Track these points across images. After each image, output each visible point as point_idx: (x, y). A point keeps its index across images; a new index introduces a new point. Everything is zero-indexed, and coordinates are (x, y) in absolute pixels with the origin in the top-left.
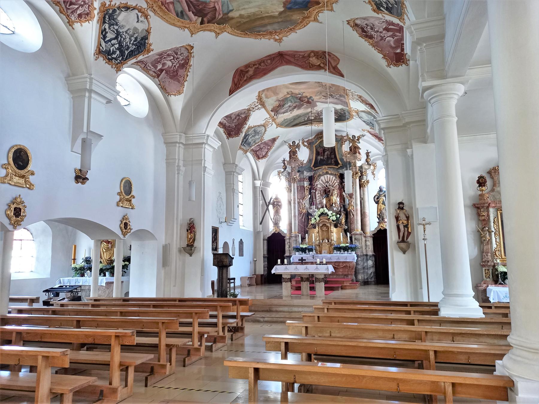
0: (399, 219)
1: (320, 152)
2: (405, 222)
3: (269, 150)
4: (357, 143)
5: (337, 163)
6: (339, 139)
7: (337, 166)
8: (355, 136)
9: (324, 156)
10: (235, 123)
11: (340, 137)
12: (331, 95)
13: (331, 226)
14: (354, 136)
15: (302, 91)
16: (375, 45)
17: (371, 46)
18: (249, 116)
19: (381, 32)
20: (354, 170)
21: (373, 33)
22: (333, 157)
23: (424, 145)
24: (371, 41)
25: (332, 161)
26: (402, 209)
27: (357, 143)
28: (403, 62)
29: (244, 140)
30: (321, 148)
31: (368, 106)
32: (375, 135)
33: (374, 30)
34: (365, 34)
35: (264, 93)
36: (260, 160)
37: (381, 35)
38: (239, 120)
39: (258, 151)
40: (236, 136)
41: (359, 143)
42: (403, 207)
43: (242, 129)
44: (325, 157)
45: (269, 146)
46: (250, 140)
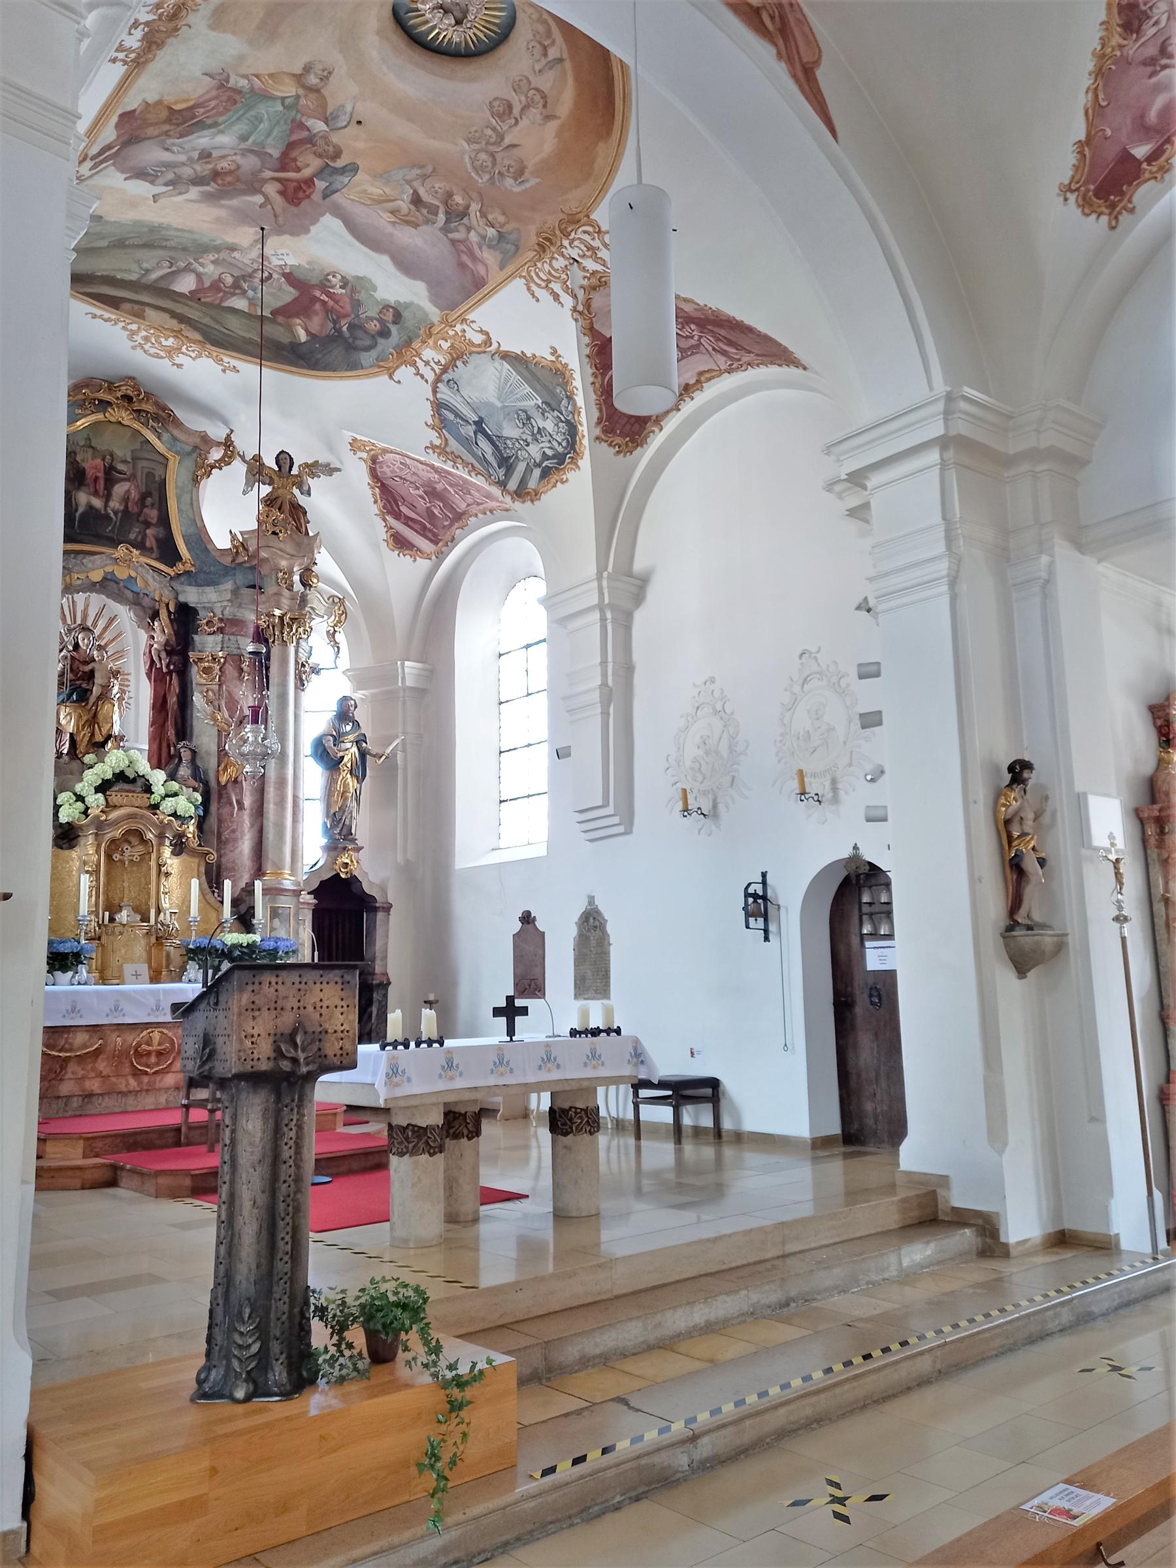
1: (90, 473)
4: (296, 491)
5: (169, 553)
7: (172, 565)
8: (291, 459)
9: (108, 498)
12: (457, 215)
13: (161, 844)
14: (284, 459)
15: (364, 109)
17: (1090, 66)
20: (285, 602)
22: (154, 521)
23: (1077, 554)
24: (1116, 40)
25: (145, 536)
27: (296, 491)
28: (1113, 206)
30: (94, 458)
31: (587, 340)
32: (389, 482)
41: (309, 494)
44: (115, 504)
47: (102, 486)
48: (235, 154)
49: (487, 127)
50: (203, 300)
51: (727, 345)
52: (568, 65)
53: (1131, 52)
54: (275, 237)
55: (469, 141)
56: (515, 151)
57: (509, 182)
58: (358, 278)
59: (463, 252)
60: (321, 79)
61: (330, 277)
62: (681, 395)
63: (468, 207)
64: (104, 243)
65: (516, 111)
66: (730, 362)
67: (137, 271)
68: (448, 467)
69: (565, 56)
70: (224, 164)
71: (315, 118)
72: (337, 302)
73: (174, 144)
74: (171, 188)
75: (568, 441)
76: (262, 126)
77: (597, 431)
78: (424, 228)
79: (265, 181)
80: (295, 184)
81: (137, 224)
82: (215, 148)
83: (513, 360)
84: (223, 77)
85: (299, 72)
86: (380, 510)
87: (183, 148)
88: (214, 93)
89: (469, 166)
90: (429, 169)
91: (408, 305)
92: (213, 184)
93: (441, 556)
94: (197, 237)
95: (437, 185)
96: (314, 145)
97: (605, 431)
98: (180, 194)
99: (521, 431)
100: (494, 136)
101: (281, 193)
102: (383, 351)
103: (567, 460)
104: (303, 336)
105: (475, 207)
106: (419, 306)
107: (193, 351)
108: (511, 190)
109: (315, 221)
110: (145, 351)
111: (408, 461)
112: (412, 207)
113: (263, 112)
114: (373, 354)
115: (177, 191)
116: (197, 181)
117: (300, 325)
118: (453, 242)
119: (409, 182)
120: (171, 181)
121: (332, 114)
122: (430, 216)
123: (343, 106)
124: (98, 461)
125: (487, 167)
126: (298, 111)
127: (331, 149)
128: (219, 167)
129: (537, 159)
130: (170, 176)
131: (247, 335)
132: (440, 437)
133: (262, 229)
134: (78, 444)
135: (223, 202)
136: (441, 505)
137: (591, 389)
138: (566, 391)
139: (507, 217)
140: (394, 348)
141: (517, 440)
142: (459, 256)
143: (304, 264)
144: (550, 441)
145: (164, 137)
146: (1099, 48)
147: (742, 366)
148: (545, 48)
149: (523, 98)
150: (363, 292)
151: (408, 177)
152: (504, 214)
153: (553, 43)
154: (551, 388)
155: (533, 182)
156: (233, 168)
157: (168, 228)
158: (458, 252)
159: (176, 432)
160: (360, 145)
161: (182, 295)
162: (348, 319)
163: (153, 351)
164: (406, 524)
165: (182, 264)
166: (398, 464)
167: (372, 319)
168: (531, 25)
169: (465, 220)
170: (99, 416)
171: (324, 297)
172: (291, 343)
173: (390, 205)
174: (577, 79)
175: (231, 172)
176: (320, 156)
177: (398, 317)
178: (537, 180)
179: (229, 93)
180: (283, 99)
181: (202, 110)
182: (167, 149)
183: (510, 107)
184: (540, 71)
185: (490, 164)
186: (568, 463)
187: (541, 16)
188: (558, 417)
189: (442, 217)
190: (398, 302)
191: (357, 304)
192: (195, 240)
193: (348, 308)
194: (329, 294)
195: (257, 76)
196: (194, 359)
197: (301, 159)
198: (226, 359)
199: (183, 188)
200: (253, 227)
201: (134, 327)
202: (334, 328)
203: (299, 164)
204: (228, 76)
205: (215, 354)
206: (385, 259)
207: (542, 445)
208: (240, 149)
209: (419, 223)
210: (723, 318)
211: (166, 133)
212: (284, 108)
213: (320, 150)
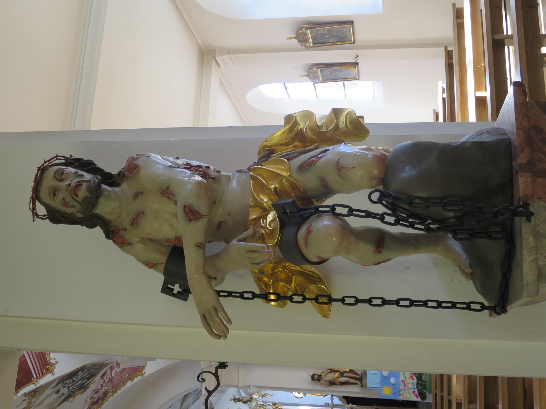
0: (332, 381)
2: (337, 374)
16: (116, 388)
19: (104, 382)
21: (102, 392)
24: (109, 394)
26: (320, 376)
33: (99, 390)
34: (100, 401)
37: (107, 381)
42: (317, 375)
53: (110, 388)
146: (112, 396)
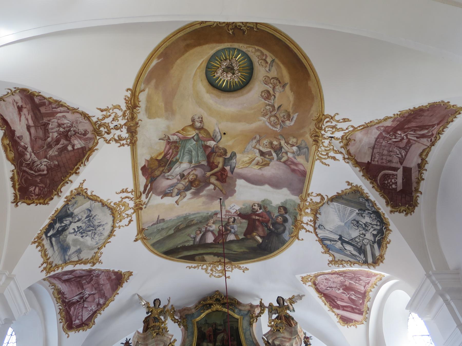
3: (100, 307)
6: (246, 312)
8: (283, 299)
10: (51, 158)
11: (248, 308)
14: (280, 300)
18: (91, 150)
27: (288, 312)
29: (58, 225)
31: (358, 169)
32: (326, 292)
35: (147, 91)
36: (72, 334)
38: (63, 155)
39: (74, 304)
40: (41, 201)
41: (294, 311)
43: (64, 185)
45: (103, 295)
46: (70, 238)
47: (212, 338)
48: (192, 170)
49: (266, 106)
50: (219, 242)
51: (421, 130)
52: (277, 60)
54: (226, 200)
55: (264, 115)
56: (282, 108)
57: (288, 123)
58: (263, 201)
59: (291, 164)
60: (201, 123)
61: (254, 207)
62: (419, 171)
63: (280, 144)
64: (172, 232)
65: (272, 92)
66: (429, 140)
67: (191, 239)
68: (341, 269)
69: (274, 58)
70: (191, 177)
71: (209, 141)
72: (262, 217)
73: (169, 176)
74: (179, 196)
75: (379, 222)
76: (193, 153)
77: (389, 208)
78: (272, 163)
79: (209, 177)
80: (219, 173)
81: (178, 217)
82: (184, 171)
83: (336, 199)
84: (167, 138)
85: (191, 123)
86: (329, 308)
87: (173, 176)
88: (168, 147)
89: (270, 126)
90: (258, 137)
91: (286, 202)
92: (193, 188)
93: (367, 319)
94: (202, 214)
95: (265, 142)
96: (216, 153)
97: (393, 207)
98: (184, 197)
99: (358, 230)
100: (271, 108)
101: (217, 180)
102: (289, 229)
103: (385, 231)
104: (260, 240)
105: (283, 142)
106: (289, 199)
107: (229, 268)
108: (290, 126)
109: (235, 185)
110: (215, 276)
111: (327, 276)
112: (262, 157)
113: (189, 147)
114: (287, 232)
115: (182, 197)
116: (187, 189)
117: (256, 235)
118: (285, 162)
119: (255, 147)
120: (178, 193)
121: (213, 135)
122: (270, 157)
123: (215, 130)
124: (210, 328)
125: (276, 122)
126: (201, 141)
127: (222, 151)
128: (190, 178)
129: (291, 106)
130: (176, 191)
131: (242, 250)
132: (330, 255)
133: (221, 199)
134: (202, 324)
135: (201, 194)
136: (353, 293)
137: (374, 190)
138: (364, 198)
139: (296, 138)
140: (292, 225)
141: (359, 236)
142: (290, 167)
143: (242, 206)
144: (372, 227)
145: (163, 174)
147: (436, 137)
148: (265, 60)
149: (271, 85)
150: (268, 206)
151: (253, 146)
152: (294, 137)
153: (266, 56)
154: (358, 201)
155: (295, 116)
156: (195, 177)
157: (190, 215)
158: (289, 165)
159: (240, 308)
160: (230, 143)
161: (211, 244)
162: (270, 222)
163: (217, 275)
164: (344, 310)
165: (204, 230)
166: (325, 281)
167: (277, 217)
168: (255, 54)
169: (283, 150)
170: (209, 311)
171: (257, 218)
172: (257, 245)
173: (254, 162)
174: (284, 63)
175: (195, 180)
176: (220, 156)
177: (285, 209)
178: (297, 114)
179: (173, 145)
180: (193, 137)
181: (168, 156)
182: (168, 179)
183: (268, 92)
184: (269, 70)
185: (276, 120)
186: (386, 231)
187: (255, 49)
188: (369, 213)
189: (274, 155)
190: (282, 203)
191: (269, 213)
192: (202, 216)
193: (267, 217)
194: (258, 215)
195: (178, 132)
196: (231, 271)
197: (215, 161)
198: (242, 266)
199: (183, 194)
200: (217, 200)
201: (205, 267)
202: (268, 229)
203: (216, 164)
204: (169, 137)
205: (237, 266)
206: (267, 187)
207: (370, 231)
208: (193, 167)
209: (269, 163)
210: (406, 115)
211: (162, 172)
212: (196, 142)
213: (219, 154)
